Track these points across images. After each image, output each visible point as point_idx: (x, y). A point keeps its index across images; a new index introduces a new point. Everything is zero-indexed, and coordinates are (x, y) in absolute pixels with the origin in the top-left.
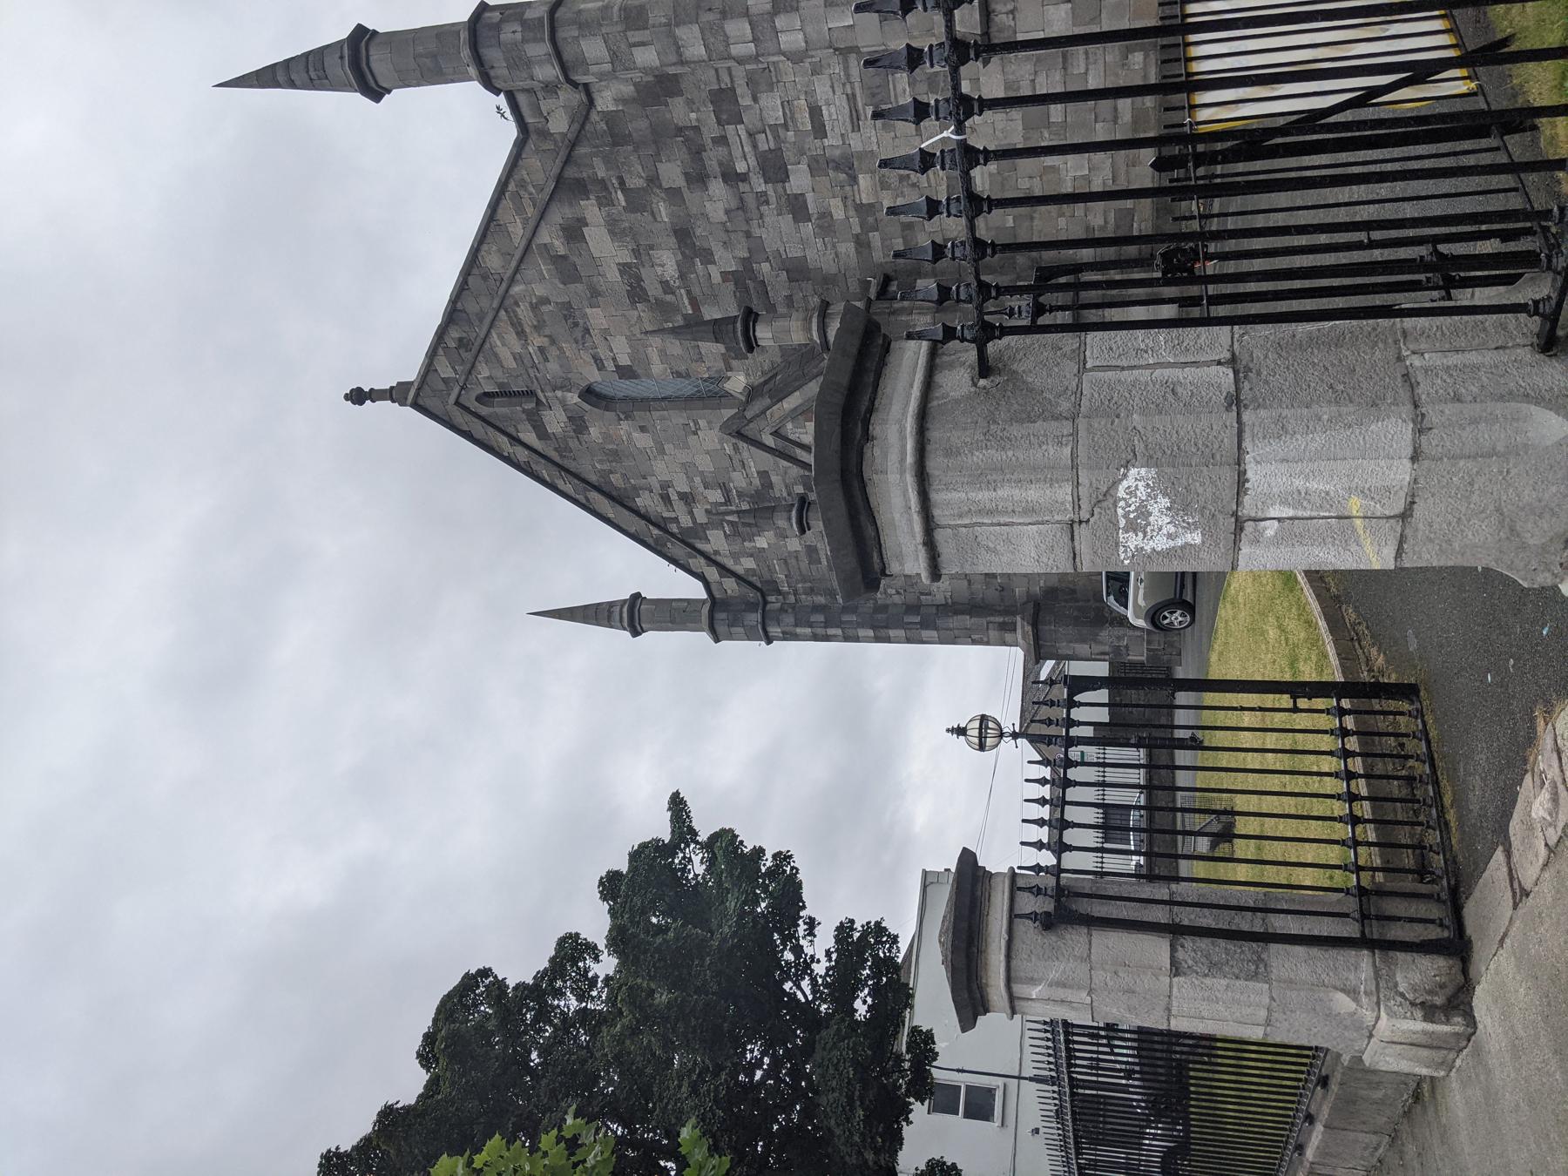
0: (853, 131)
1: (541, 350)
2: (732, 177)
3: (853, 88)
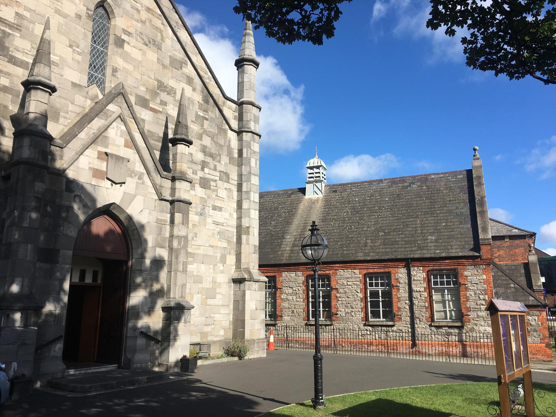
0: (213, 221)
1: (138, 11)
2: (204, 165)
3: (225, 226)
